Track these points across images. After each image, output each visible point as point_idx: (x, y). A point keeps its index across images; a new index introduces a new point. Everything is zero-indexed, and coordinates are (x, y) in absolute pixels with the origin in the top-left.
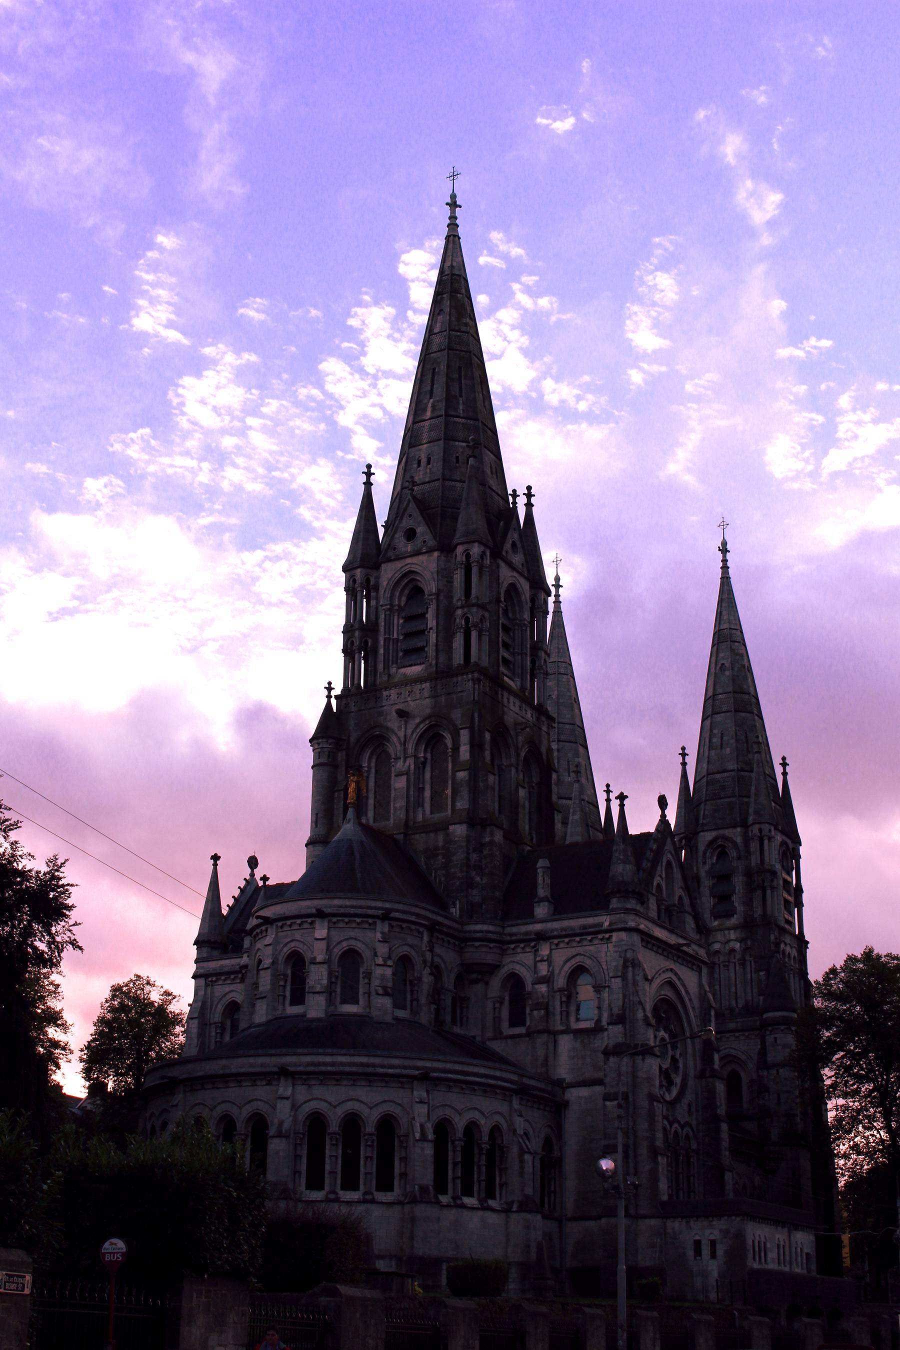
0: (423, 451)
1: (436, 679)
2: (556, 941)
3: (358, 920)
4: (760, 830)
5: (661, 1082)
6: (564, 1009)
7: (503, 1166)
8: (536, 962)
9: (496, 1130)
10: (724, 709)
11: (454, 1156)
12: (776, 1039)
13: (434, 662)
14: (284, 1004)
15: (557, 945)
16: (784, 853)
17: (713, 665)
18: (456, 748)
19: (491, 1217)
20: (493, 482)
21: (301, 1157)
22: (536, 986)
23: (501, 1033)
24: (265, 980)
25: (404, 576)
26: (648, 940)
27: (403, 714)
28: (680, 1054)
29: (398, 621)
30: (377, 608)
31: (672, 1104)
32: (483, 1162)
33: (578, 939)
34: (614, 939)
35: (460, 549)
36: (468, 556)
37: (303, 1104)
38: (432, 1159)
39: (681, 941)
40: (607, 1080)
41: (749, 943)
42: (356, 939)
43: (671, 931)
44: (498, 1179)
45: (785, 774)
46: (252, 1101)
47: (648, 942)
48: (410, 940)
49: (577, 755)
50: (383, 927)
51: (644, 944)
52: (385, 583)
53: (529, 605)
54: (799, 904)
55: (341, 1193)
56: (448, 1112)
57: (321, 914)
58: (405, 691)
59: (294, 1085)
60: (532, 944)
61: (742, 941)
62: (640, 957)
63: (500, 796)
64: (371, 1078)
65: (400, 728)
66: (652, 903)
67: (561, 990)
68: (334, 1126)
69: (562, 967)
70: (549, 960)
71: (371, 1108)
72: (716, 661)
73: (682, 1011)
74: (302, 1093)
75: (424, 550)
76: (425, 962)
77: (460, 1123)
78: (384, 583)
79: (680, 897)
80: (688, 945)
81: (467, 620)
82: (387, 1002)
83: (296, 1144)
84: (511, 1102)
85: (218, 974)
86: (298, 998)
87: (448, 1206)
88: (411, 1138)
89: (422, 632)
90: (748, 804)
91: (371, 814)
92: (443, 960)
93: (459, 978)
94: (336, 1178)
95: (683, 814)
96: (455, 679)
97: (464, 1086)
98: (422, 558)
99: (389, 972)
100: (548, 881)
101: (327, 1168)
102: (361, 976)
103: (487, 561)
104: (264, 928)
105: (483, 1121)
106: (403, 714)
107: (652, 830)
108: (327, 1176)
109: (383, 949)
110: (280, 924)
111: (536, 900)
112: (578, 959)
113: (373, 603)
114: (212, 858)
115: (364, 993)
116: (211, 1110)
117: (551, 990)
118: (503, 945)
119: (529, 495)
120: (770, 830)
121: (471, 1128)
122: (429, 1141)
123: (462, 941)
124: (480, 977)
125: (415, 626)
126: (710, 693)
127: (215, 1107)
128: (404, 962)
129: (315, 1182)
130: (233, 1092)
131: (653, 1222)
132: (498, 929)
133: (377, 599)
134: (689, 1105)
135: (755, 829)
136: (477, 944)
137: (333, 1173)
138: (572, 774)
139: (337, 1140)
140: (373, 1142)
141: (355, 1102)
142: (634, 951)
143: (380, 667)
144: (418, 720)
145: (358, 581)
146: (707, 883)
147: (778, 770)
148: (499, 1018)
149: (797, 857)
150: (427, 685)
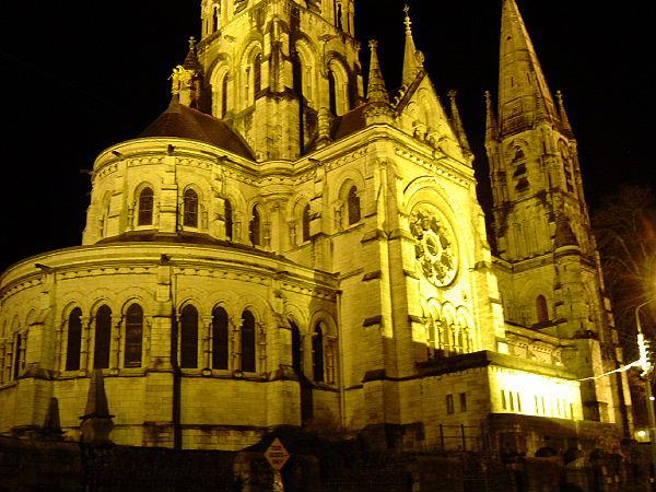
44: (257, 354)
94: (88, 358)
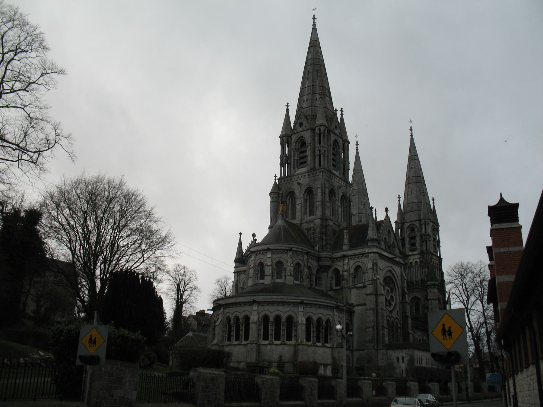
0: (305, 98)
1: (310, 172)
2: (350, 257)
3: (282, 251)
4: (425, 221)
5: (386, 304)
6: (353, 280)
7: (331, 333)
8: (343, 264)
9: (328, 321)
10: (413, 182)
11: (313, 329)
12: (431, 291)
13: (309, 166)
14: (258, 280)
15: (350, 258)
16: (433, 229)
17: (408, 168)
19: (327, 350)
20: (329, 106)
21: (261, 330)
22: (343, 273)
23: (332, 288)
24: (251, 272)
25: (299, 138)
26: (381, 256)
27: (298, 183)
28: (394, 295)
30: (291, 150)
31: (391, 312)
32: (324, 331)
33: (357, 256)
34: (369, 256)
35: (317, 128)
36: (320, 130)
37: (261, 312)
38: (305, 330)
39: (393, 257)
40: (367, 304)
41: (422, 259)
42: (280, 257)
43: (390, 253)
45: (433, 203)
46: (245, 311)
47: (381, 257)
48: (300, 258)
49: (365, 199)
50: (290, 253)
51: (380, 257)
53: (342, 147)
54: (439, 246)
55: (274, 341)
56: (311, 314)
57: (269, 249)
58: (300, 176)
59: (258, 306)
60: (342, 259)
61: (420, 258)
62: (378, 262)
63: (332, 210)
64: (284, 303)
65: (298, 188)
66: (383, 244)
67: (352, 274)
68: (272, 319)
69: (352, 266)
70: (348, 264)
71: (284, 313)
72: (409, 166)
74: (261, 308)
75: (305, 129)
76: (305, 265)
77: (315, 318)
78: (293, 141)
79: (393, 242)
80: (396, 258)
81: (320, 152)
82: (292, 278)
83: (259, 326)
84: (333, 311)
85: (241, 272)
86: (262, 277)
87: (311, 346)
88: (298, 323)
90: (421, 213)
91: (290, 217)
92: (312, 264)
93: (318, 270)
94: (272, 337)
95: (399, 217)
96: (316, 172)
97: (316, 306)
98: (305, 132)
99: (292, 268)
100: (347, 237)
101: (270, 333)
103: (326, 132)
104: (251, 255)
105: (323, 317)
107: (383, 220)
108: (269, 336)
109: (290, 261)
110: (256, 253)
111: (344, 244)
112: (357, 263)
113: (290, 148)
114: (239, 234)
115: (284, 275)
116: (232, 314)
117: (349, 274)
118: (333, 260)
119: (342, 111)
120: (428, 222)
121: (319, 320)
122: (303, 324)
123: (319, 259)
124: (325, 270)
126: (408, 177)
127: (233, 313)
128: (298, 265)
129: (266, 338)
130: (238, 309)
131: (383, 351)
132: (331, 254)
133: (291, 146)
134: (397, 312)
135: (423, 221)
136: (323, 259)
137: (271, 335)
138: (363, 206)
139: (273, 324)
140: (285, 324)
141: (279, 311)
142: (376, 260)
143: (292, 168)
144: (304, 185)
145: (285, 141)
146: (407, 240)
147: (431, 202)
148: (332, 283)
149: (438, 231)
150: (307, 174)
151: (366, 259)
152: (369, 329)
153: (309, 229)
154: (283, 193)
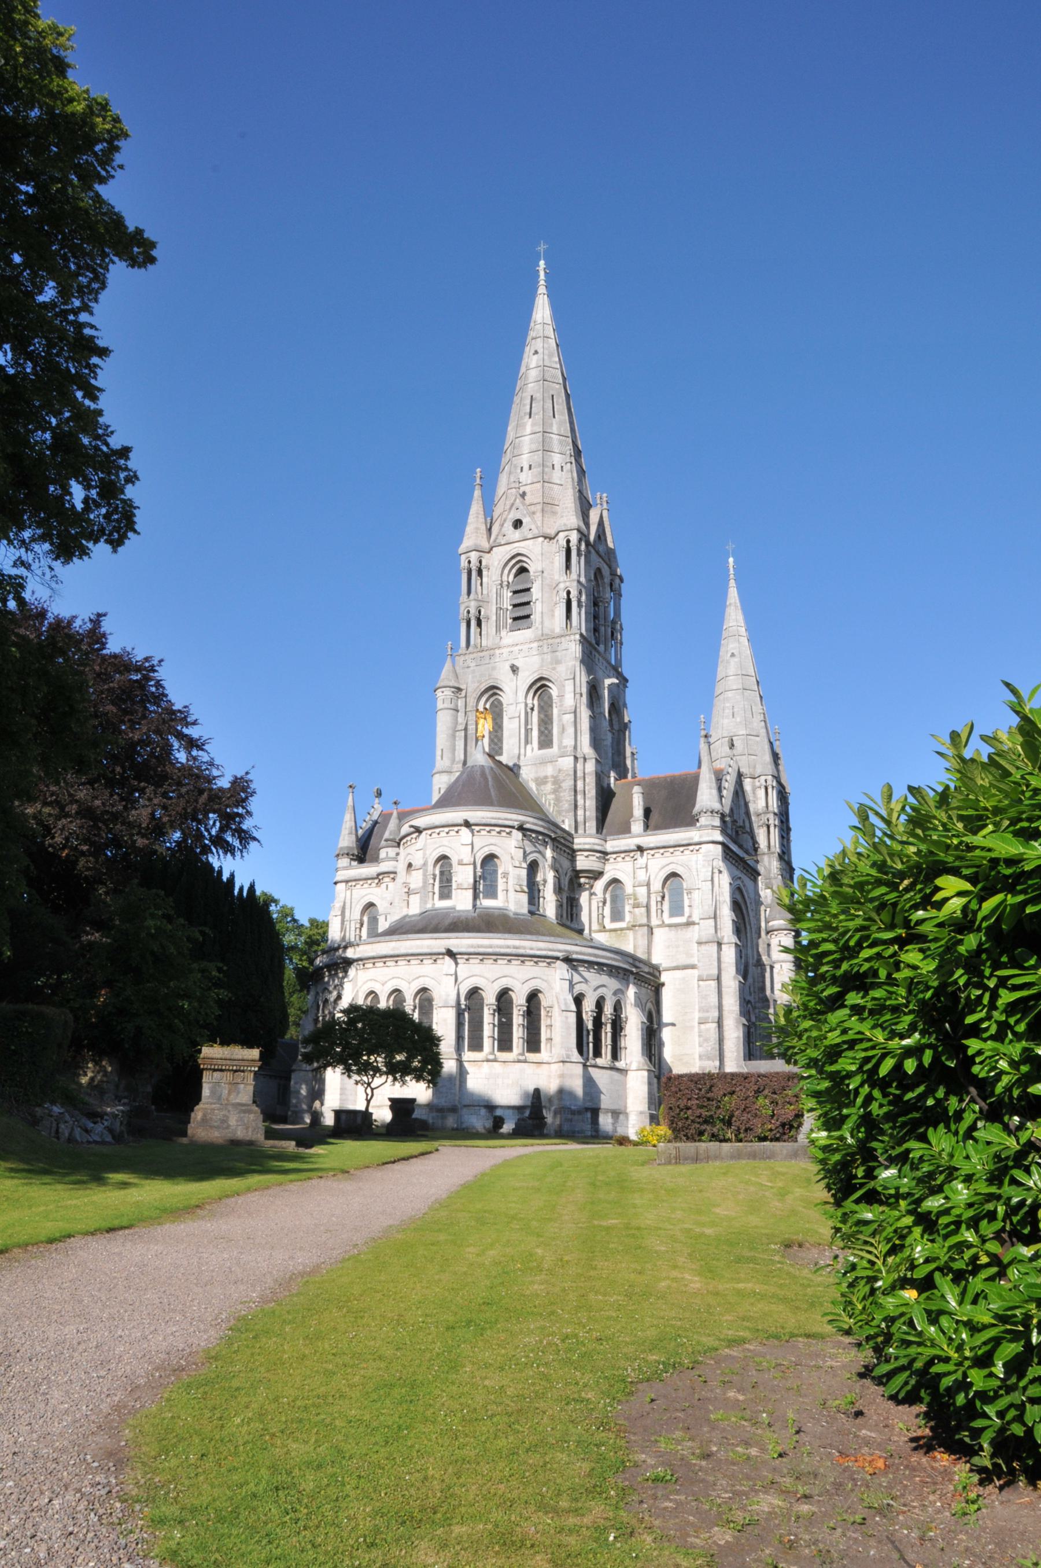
2: (652, 852)
18: (561, 696)
25: (513, 557)
27: (514, 669)
29: (508, 594)
40: (699, 965)
43: (741, 847)
52: (496, 563)
64: (523, 957)
73: (745, 911)
75: (530, 536)
86: (445, 893)
89: (528, 603)
102: (499, 876)
106: (514, 669)
125: (522, 598)
132: (602, 842)
150: (535, 645)
151: (694, 857)
152: (708, 1026)
153: (541, 781)
154: (469, 690)
